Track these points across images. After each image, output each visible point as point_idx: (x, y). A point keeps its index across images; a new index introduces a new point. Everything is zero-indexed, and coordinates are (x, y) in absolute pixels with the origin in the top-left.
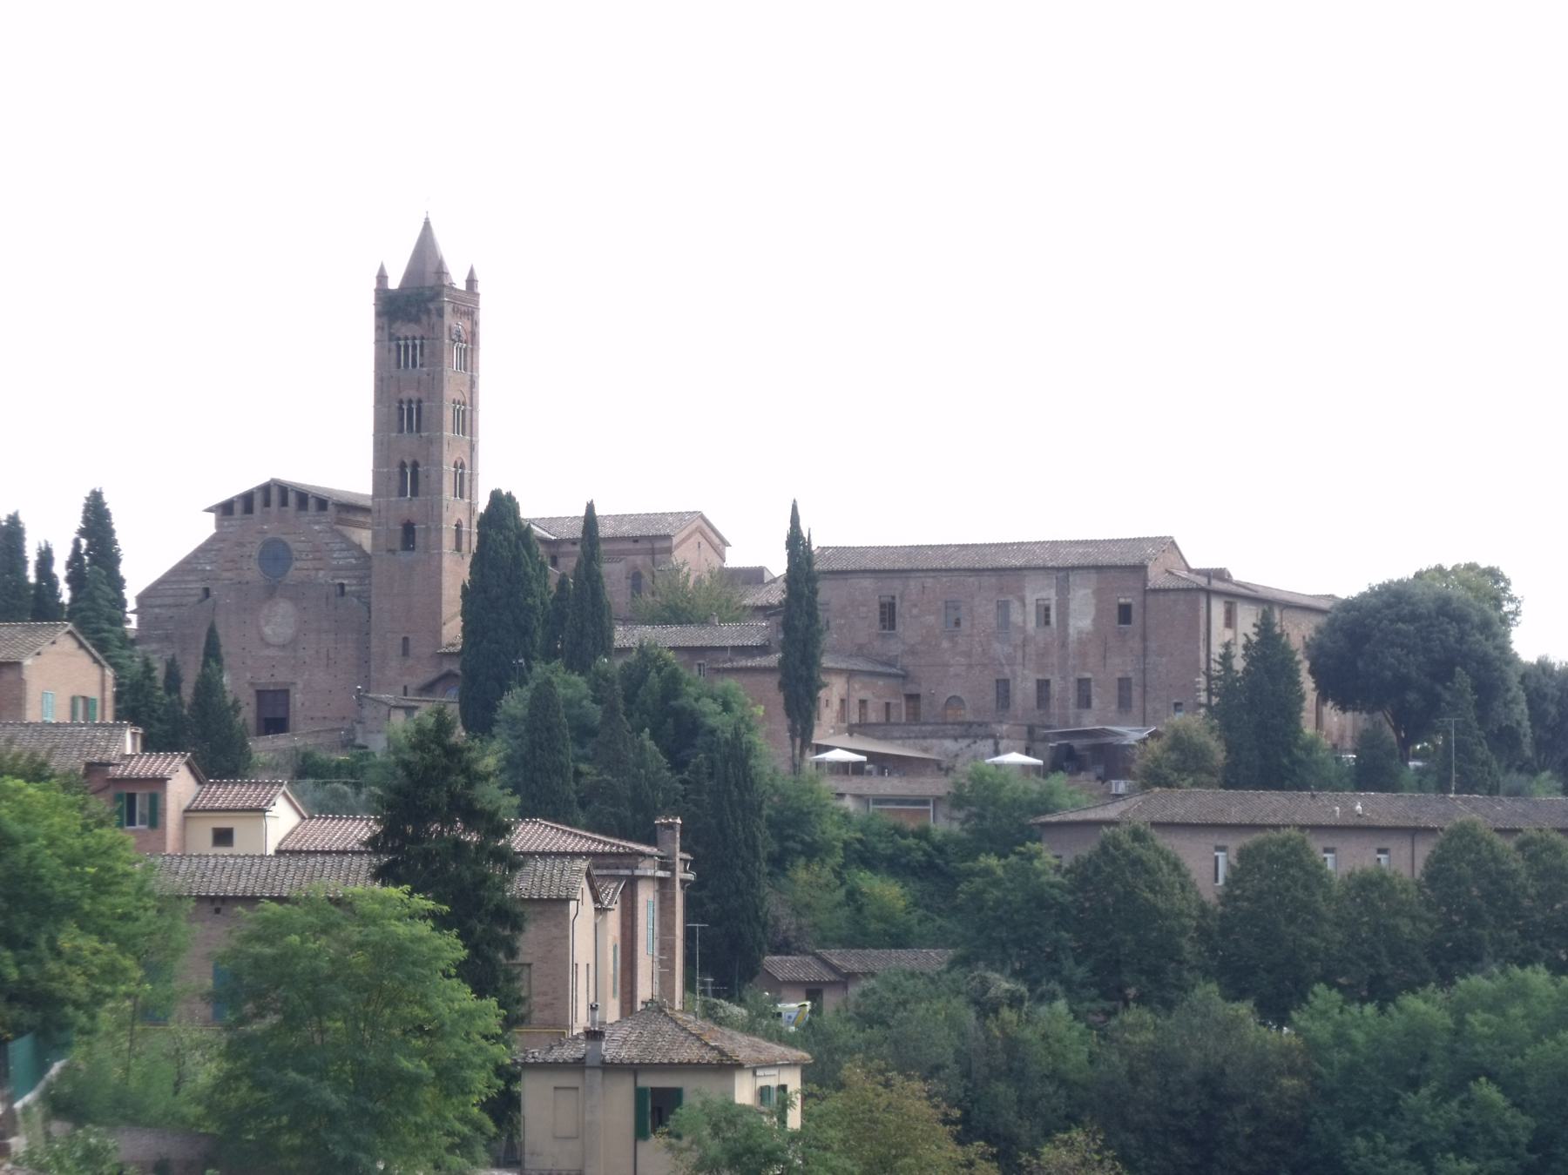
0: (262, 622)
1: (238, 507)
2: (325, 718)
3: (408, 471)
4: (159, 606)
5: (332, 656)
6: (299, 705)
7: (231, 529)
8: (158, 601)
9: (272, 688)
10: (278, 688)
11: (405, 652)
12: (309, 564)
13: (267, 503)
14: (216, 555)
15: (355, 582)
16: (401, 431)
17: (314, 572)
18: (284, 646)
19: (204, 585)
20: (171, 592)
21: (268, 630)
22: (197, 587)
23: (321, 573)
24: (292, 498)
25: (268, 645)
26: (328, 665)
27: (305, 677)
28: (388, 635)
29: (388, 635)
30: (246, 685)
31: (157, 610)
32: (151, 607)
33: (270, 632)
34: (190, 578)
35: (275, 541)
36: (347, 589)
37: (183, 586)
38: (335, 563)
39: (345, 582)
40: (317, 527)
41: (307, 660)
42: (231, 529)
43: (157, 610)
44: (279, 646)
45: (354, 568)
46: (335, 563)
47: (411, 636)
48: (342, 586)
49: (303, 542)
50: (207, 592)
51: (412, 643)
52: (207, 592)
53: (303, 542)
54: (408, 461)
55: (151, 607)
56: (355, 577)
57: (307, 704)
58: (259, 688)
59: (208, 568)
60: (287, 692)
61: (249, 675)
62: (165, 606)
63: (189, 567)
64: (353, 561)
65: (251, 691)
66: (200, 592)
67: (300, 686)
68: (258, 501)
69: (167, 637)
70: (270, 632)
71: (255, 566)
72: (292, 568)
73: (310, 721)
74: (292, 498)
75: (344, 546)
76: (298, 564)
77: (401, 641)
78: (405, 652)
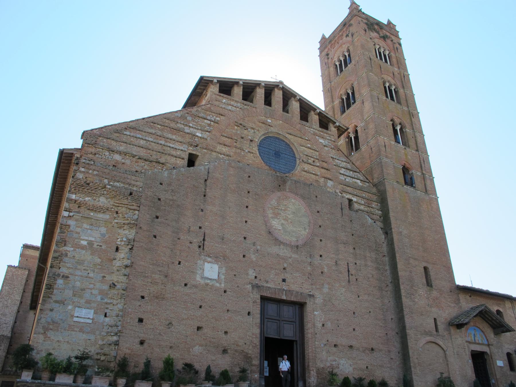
0: (270, 213)
1: (238, 91)
2: (351, 347)
3: (398, 128)
4: (120, 153)
5: (353, 271)
6: (320, 325)
7: (230, 107)
8: (122, 148)
9: (284, 297)
10: (293, 299)
11: (429, 283)
12: (318, 171)
13: (268, 102)
14: (209, 125)
15: (363, 202)
16: (387, 97)
17: (323, 179)
18: (297, 247)
19: (191, 150)
20: (142, 142)
21: (276, 224)
22: (185, 150)
23: (330, 183)
24: (295, 106)
25: (278, 242)
26: (349, 281)
27: (326, 290)
28: (411, 261)
29: (411, 261)
30: (249, 287)
31: (117, 157)
32: (112, 151)
33: (280, 228)
34: (174, 137)
35: (277, 139)
36: (356, 206)
37: (163, 142)
38: (342, 178)
39: (354, 199)
40: (321, 141)
41: (326, 270)
42: (230, 107)
43: (117, 157)
44: (292, 247)
45: (361, 189)
46: (342, 178)
47: (430, 267)
48: (350, 201)
49: (309, 148)
50: (191, 161)
51: (432, 273)
52: (191, 161)
53: (309, 148)
54: (397, 121)
55: (112, 151)
56: (363, 198)
57: (329, 325)
58: (265, 294)
59: (198, 134)
60: (301, 305)
61: (252, 274)
62: (134, 156)
63: (173, 125)
64: (359, 181)
65: (257, 297)
66: (186, 157)
67: (319, 300)
68: (260, 93)
69: (131, 194)
70: (280, 228)
71: (255, 149)
72: (298, 168)
73: (334, 349)
74: (295, 106)
75: (349, 166)
76: (307, 167)
77: (423, 270)
78: (429, 283)
